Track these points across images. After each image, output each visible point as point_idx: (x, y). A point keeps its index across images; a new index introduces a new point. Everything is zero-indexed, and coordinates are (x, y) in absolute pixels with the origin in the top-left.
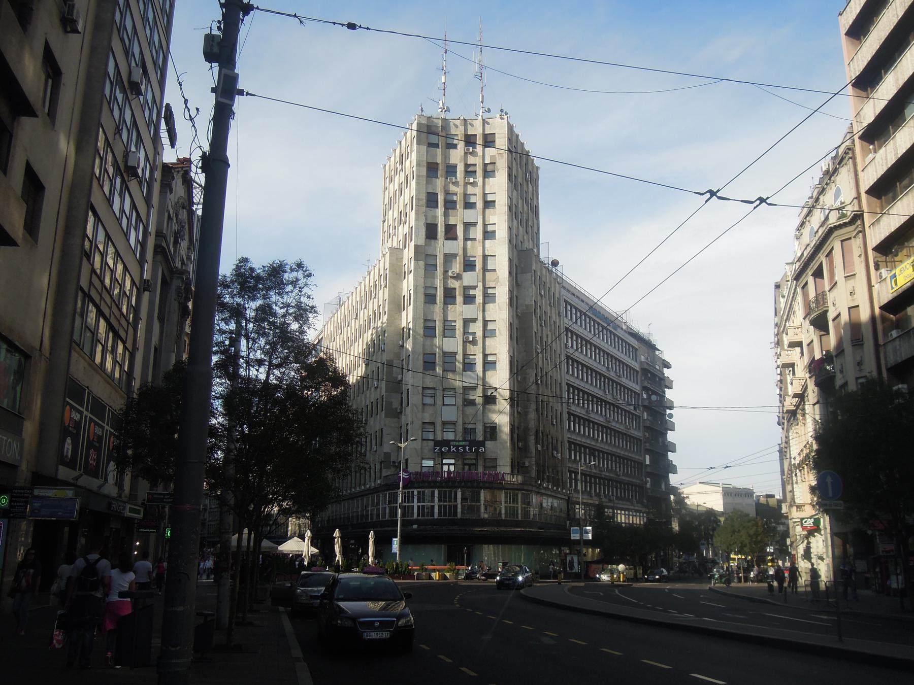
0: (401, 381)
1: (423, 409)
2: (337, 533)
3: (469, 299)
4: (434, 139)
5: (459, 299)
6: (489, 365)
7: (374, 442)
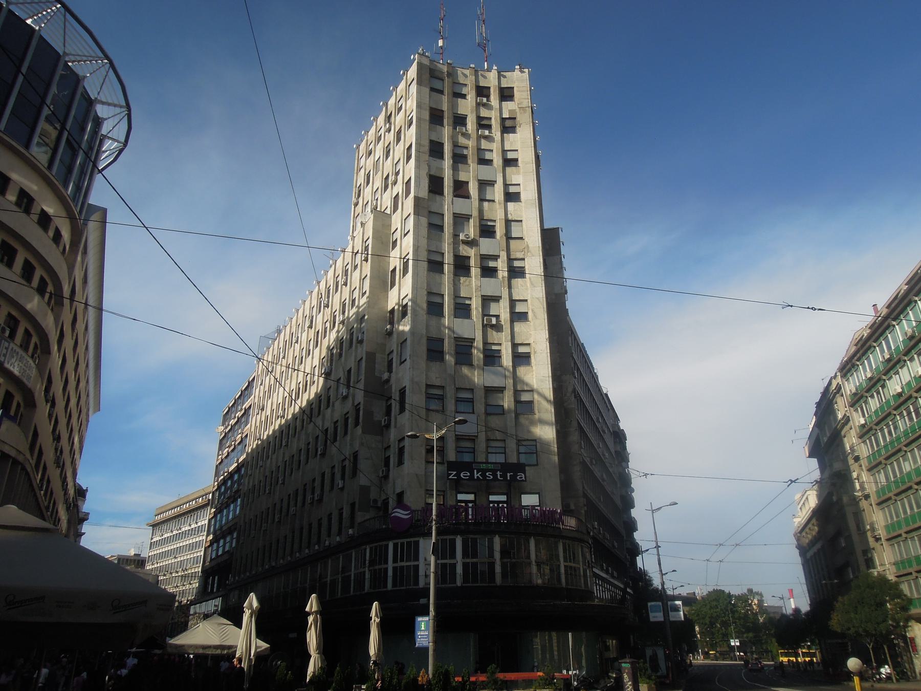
0: (388, 381)
1: (427, 415)
2: (312, 604)
3: (489, 272)
4: (437, 85)
5: (475, 271)
6: (520, 359)
7: (338, 475)
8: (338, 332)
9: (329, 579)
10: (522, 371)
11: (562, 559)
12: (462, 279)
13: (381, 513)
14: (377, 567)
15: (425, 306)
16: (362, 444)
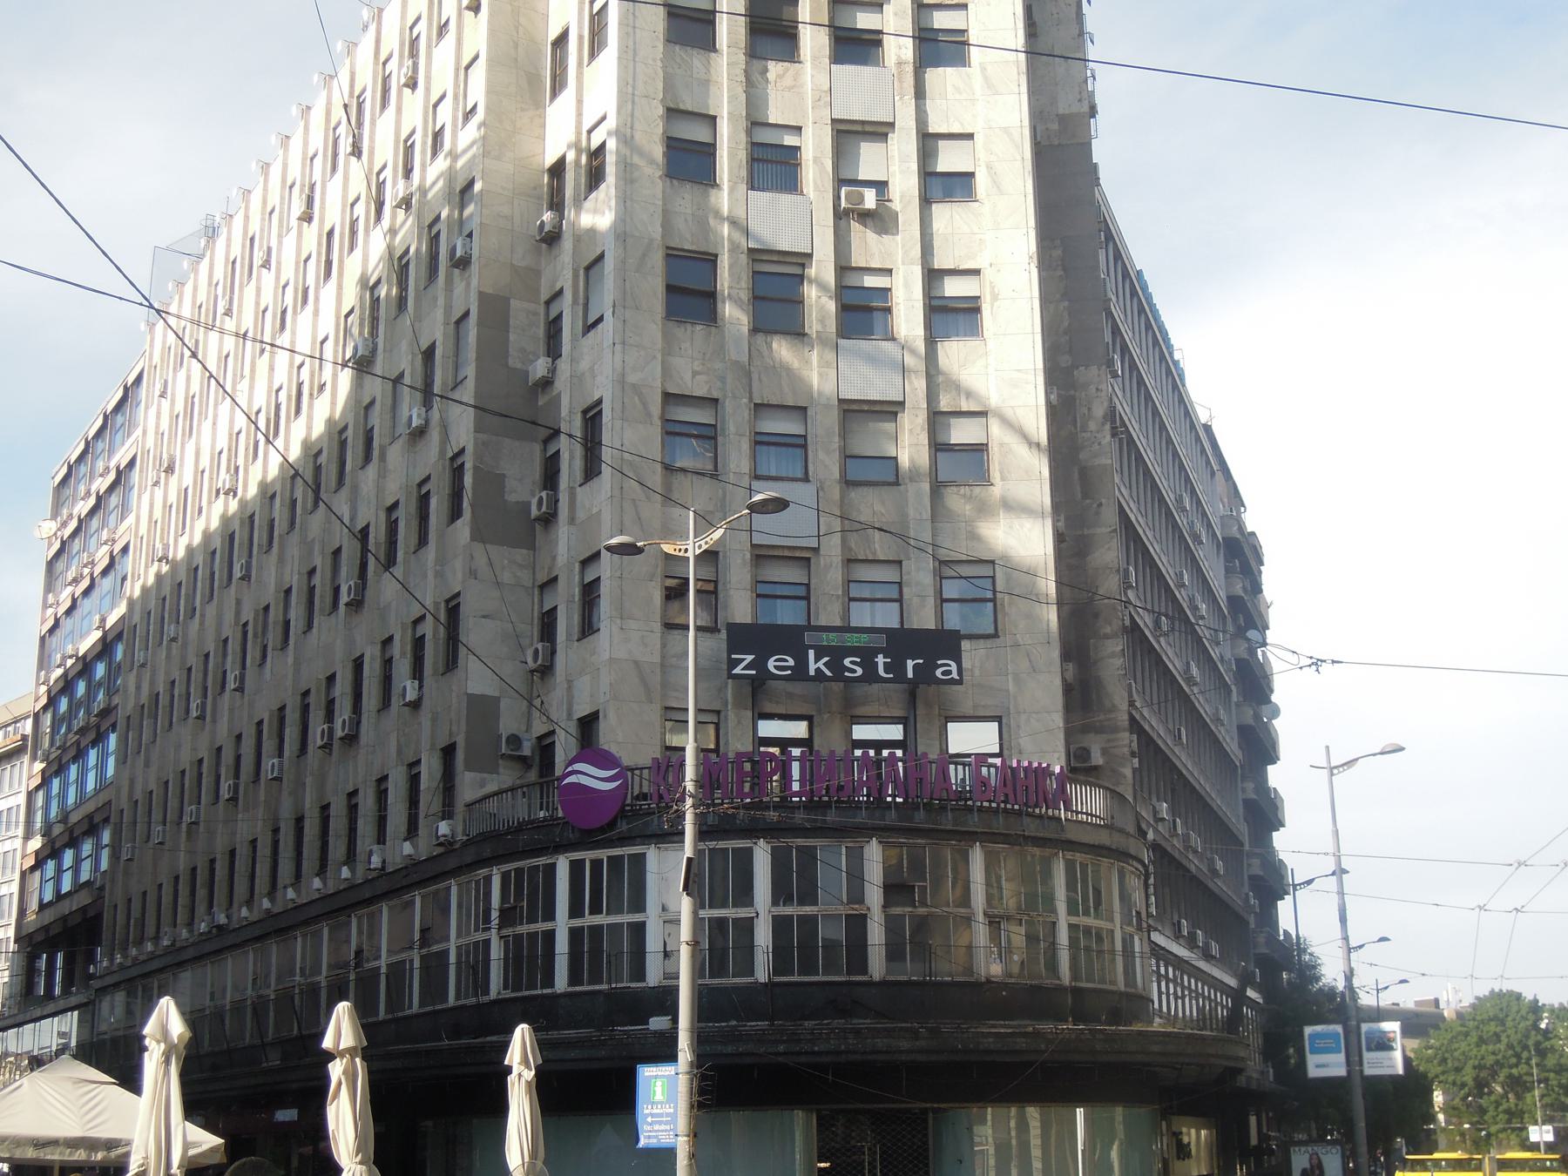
0: (547, 383)
1: (668, 486)
2: (341, 1028)
5: (813, 41)
6: (951, 315)
7: (402, 667)
8: (393, 231)
9: (383, 963)
10: (953, 353)
11: (1061, 907)
12: (774, 69)
13: (533, 776)
14: (524, 929)
15: (658, 151)
16: (473, 573)
